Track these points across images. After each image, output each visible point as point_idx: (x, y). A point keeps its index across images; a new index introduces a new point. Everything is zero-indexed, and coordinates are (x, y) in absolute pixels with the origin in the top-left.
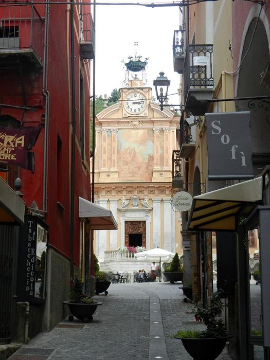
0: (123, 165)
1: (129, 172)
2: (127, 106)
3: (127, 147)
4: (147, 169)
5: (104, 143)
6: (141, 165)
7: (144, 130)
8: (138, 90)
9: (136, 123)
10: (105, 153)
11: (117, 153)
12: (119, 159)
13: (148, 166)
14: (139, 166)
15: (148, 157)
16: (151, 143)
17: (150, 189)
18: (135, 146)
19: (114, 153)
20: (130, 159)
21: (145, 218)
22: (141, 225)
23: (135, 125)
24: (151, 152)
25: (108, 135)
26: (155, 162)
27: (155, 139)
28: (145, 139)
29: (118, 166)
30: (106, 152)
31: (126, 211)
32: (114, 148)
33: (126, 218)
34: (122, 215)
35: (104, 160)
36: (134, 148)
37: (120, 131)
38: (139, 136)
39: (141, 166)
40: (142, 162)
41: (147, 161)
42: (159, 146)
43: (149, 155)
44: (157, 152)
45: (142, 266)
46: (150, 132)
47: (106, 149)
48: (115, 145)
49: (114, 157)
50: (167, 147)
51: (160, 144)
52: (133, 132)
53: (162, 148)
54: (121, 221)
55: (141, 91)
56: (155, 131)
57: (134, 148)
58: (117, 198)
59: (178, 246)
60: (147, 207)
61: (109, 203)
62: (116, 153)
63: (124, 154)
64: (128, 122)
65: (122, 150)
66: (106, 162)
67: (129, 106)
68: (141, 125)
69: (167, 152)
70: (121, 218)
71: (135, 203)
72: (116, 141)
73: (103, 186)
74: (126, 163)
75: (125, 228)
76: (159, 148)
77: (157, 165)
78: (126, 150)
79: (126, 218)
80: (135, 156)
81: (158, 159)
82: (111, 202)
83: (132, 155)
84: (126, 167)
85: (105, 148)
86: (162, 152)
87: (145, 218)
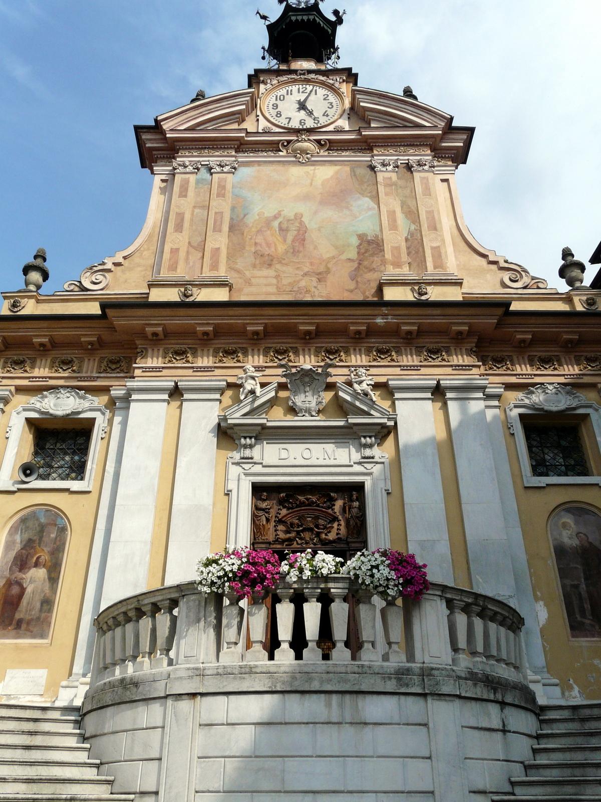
0: (254, 266)
1: (278, 288)
2: (274, 112)
3: (269, 212)
4: (353, 278)
5: (182, 201)
6: (330, 266)
7: (338, 168)
8: (313, 76)
9: (306, 145)
10: (179, 228)
11: (232, 228)
12: (236, 250)
13: (358, 269)
14: (322, 269)
15: (355, 241)
16: (366, 202)
17: (374, 342)
18: (303, 209)
19: (217, 229)
20: (281, 248)
21: (358, 468)
22: (339, 504)
23: (304, 152)
24: (367, 226)
25: (198, 182)
26: (388, 255)
27: (381, 189)
28: (342, 191)
29: (231, 268)
30: (186, 225)
31: (263, 434)
32: (220, 214)
33: (258, 469)
34: (237, 456)
35: (175, 251)
36: (298, 217)
37: (243, 172)
38: (318, 181)
39: (328, 271)
40: (333, 258)
41: (353, 254)
42: (398, 210)
43: (361, 237)
44: (394, 226)
45: (413, 741)
46: (364, 172)
47: (187, 217)
48: (222, 206)
49: (219, 241)
50: (430, 213)
51: (403, 205)
52: (296, 171)
53: (413, 215)
54: (232, 485)
55: (321, 78)
56: (379, 167)
57: (298, 217)
58: (219, 377)
59: (549, 620)
60: (369, 414)
61: (175, 404)
62: (226, 228)
63: (259, 231)
64: (274, 147)
65: (251, 220)
66: (182, 254)
67: (279, 114)
68: (326, 153)
69: (434, 227)
70: (234, 471)
71: (306, 399)
72: (229, 195)
73: (155, 324)
74: (268, 261)
75: (255, 518)
76: (400, 217)
77: (397, 265)
78: (268, 222)
79: (258, 469)
80: (301, 237)
81: (398, 249)
82: (186, 396)
83: (290, 238)
84: (265, 272)
85: (180, 217)
86: (413, 227)
87: (358, 468)
